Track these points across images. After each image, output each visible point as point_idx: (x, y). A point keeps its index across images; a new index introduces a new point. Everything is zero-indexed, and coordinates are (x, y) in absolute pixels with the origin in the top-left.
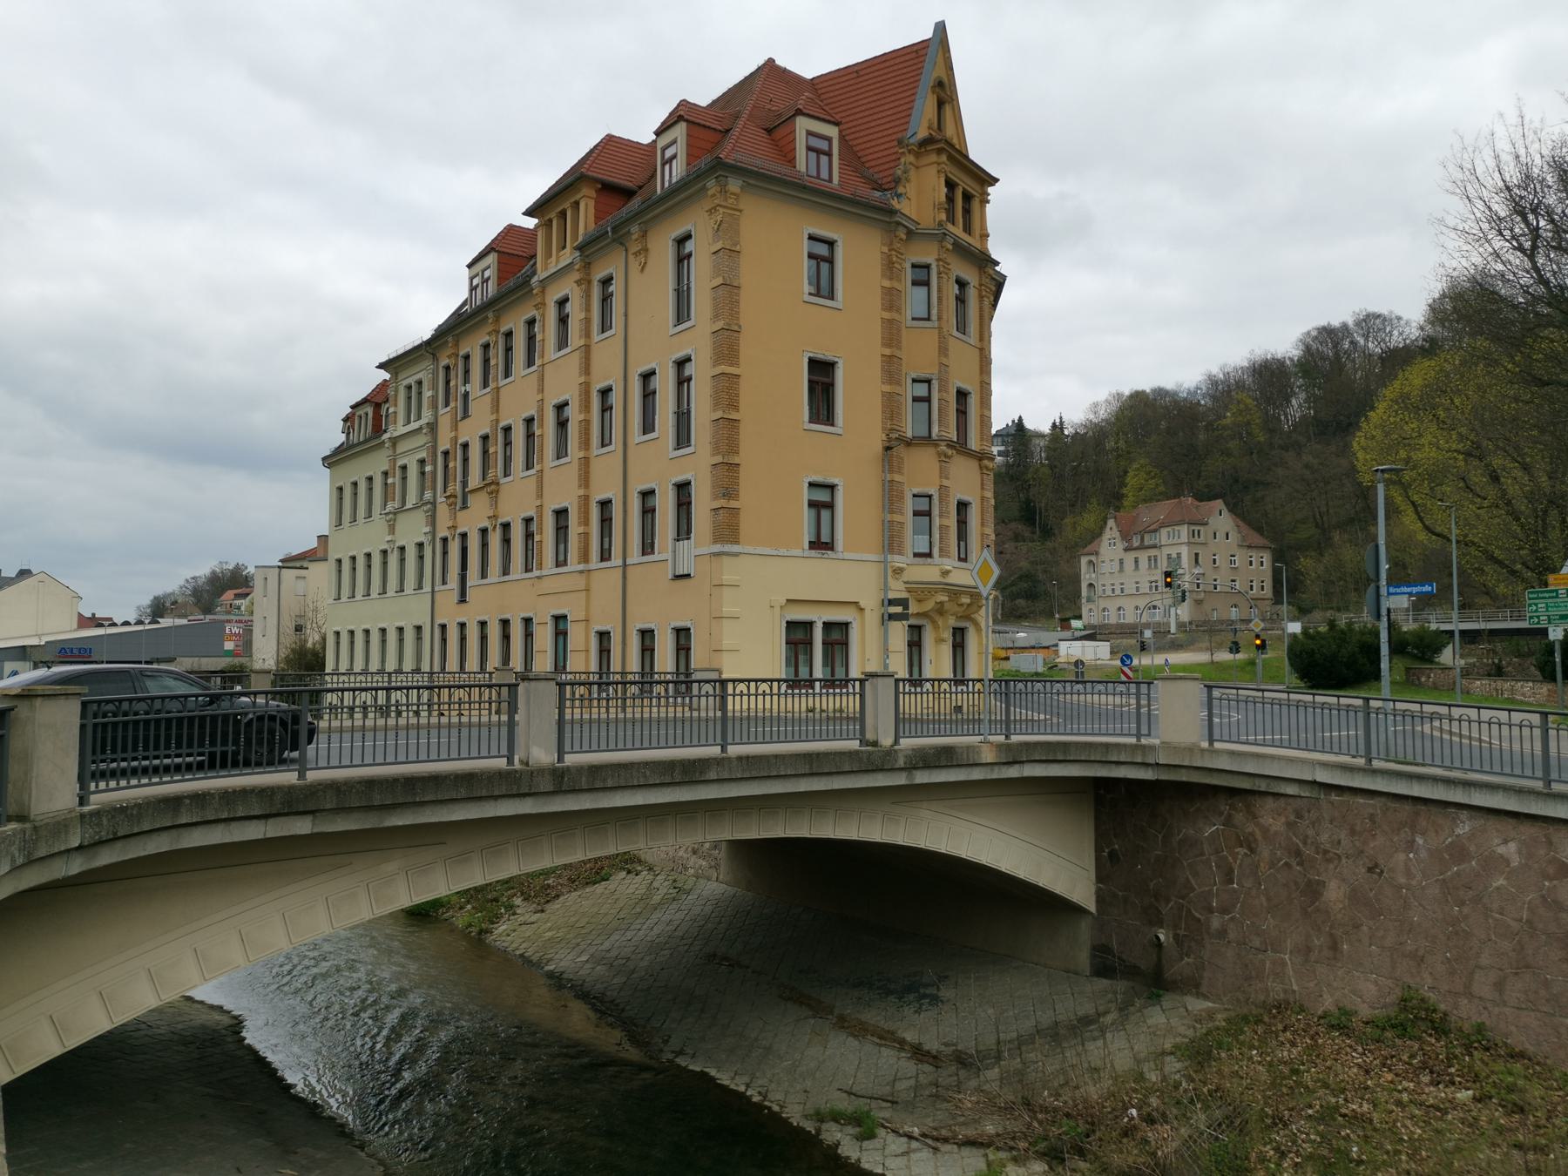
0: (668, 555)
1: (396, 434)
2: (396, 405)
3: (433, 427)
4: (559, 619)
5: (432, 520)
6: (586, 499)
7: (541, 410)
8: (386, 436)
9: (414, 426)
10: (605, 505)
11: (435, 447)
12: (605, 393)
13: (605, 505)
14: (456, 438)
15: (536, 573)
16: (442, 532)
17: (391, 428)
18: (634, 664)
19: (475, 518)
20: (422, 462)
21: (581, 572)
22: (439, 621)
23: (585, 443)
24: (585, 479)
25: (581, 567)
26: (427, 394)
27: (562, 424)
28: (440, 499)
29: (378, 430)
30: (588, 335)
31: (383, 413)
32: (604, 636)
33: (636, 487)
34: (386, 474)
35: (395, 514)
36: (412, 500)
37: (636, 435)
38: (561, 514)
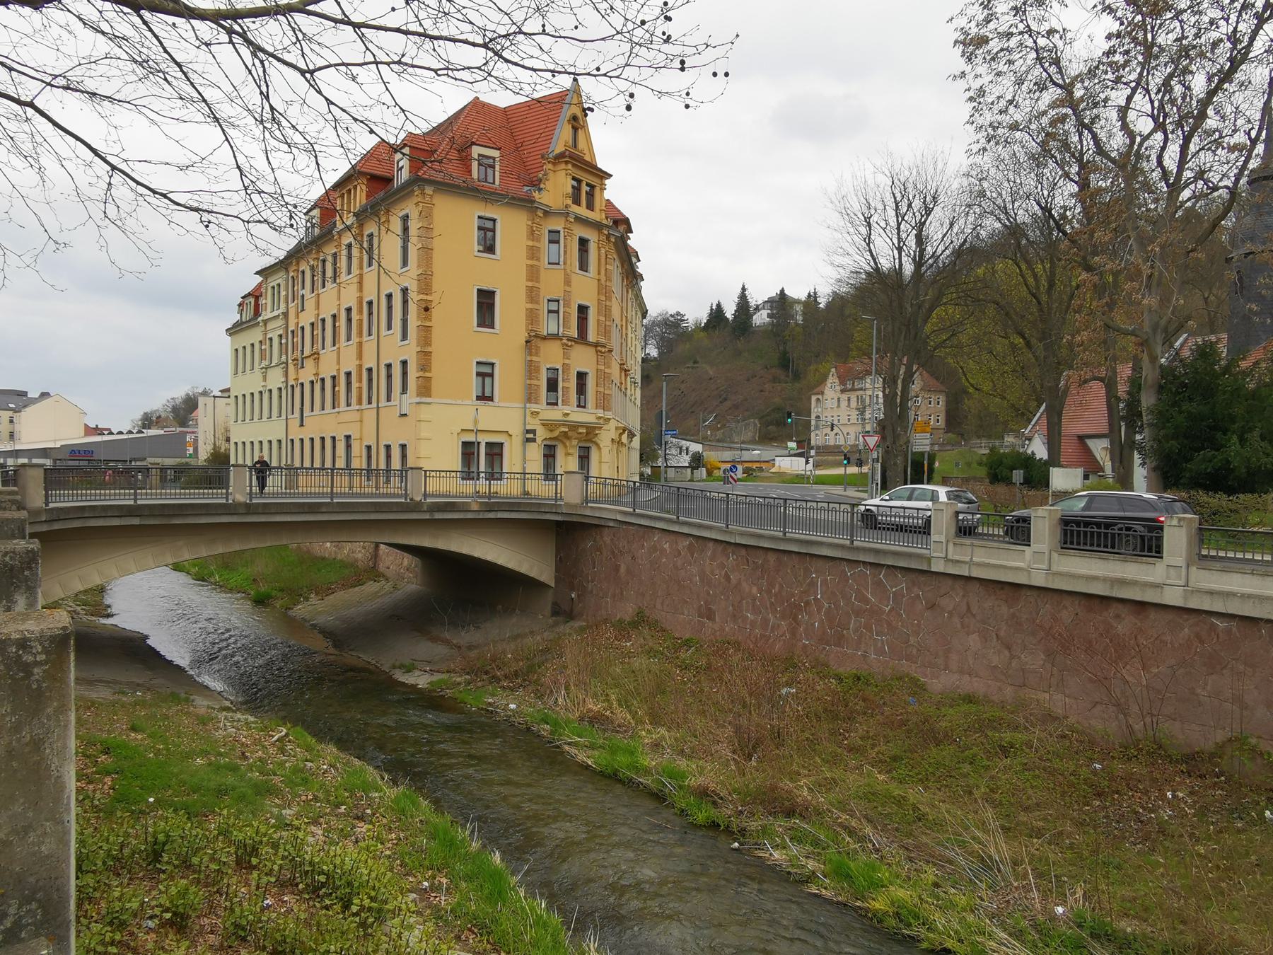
0: (397, 403)
1: (266, 318)
2: (266, 299)
3: (286, 315)
4: (348, 438)
5: (286, 375)
6: (360, 366)
7: (339, 310)
8: (260, 319)
9: (276, 313)
10: (370, 370)
11: (287, 328)
12: (370, 303)
13: (370, 370)
14: (298, 323)
15: (337, 410)
16: (291, 382)
17: (264, 313)
18: (383, 466)
19: (307, 375)
20: (280, 336)
21: (358, 410)
22: (290, 438)
23: (360, 334)
24: (360, 356)
25: (357, 407)
26: (283, 293)
27: (349, 320)
28: (290, 361)
29: (257, 313)
30: (361, 268)
31: (260, 303)
32: (369, 448)
33: (384, 362)
34: (261, 342)
35: (266, 368)
36: (275, 361)
37: (384, 332)
38: (348, 374)
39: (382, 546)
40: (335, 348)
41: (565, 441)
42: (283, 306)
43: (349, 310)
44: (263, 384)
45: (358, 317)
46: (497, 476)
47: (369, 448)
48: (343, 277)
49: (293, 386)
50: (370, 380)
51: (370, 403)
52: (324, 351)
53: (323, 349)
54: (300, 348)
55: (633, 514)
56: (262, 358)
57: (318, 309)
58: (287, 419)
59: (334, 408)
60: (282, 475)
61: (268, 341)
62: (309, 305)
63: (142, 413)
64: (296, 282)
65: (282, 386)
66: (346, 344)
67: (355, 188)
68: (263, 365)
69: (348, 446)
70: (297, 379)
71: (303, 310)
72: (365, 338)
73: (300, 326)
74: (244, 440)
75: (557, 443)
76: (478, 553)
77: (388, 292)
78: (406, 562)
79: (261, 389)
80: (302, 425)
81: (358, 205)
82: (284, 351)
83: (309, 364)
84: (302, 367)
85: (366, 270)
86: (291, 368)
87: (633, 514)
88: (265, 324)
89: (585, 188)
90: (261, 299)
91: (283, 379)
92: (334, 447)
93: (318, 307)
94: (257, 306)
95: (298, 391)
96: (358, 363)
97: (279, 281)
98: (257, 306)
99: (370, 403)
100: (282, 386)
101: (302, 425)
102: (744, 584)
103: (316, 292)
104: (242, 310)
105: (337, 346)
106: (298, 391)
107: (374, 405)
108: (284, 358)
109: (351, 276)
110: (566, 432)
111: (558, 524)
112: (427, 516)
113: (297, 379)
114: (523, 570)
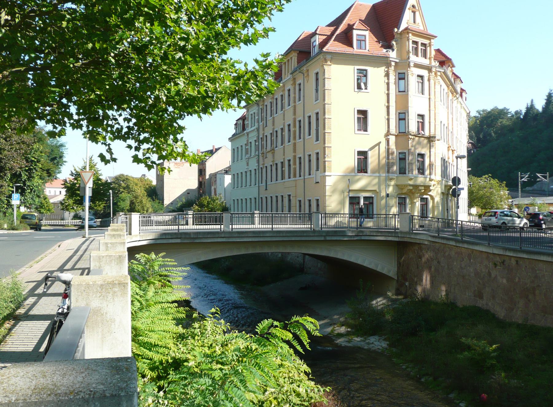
0: (314, 176)
1: (248, 131)
2: (248, 121)
3: (258, 129)
4: (289, 196)
5: (258, 162)
6: (295, 157)
7: (284, 126)
8: (245, 132)
9: (253, 128)
10: (300, 158)
11: (258, 136)
12: (300, 121)
13: (300, 158)
15: (283, 181)
16: (261, 166)
17: (247, 129)
18: (307, 212)
19: (268, 162)
20: (255, 141)
21: (294, 180)
22: (260, 196)
23: (295, 138)
24: (295, 150)
25: (294, 179)
26: (256, 118)
27: (289, 130)
28: (260, 155)
29: (244, 129)
30: (295, 102)
31: (245, 123)
32: (300, 201)
33: (307, 154)
34: (246, 144)
35: (248, 159)
36: (253, 154)
37: (307, 137)
38: (289, 161)
39: (307, 256)
40: (282, 146)
41: (411, 195)
42: (256, 124)
43: (289, 125)
44: (247, 167)
45: (293, 129)
46: (371, 216)
47: (300, 201)
48: (286, 107)
49: (262, 168)
50: (300, 163)
51: (300, 176)
52: (277, 148)
53: (277, 147)
54: (265, 147)
55: (438, 237)
56: (247, 153)
57: (274, 125)
58: (259, 186)
59: (282, 179)
60: (259, 217)
61: (249, 144)
62: (270, 123)
63: (500, 107)
64: (272, 105)
65: (256, 168)
66: (288, 144)
67: (291, 58)
68: (247, 157)
69: (290, 200)
70: (264, 164)
71: (266, 126)
72: (298, 140)
73: (265, 135)
74: (238, 198)
75: (406, 196)
76: (353, 259)
77: (308, 115)
78: (319, 265)
79: (246, 170)
80: (266, 189)
81: (293, 68)
82: (257, 149)
83: (270, 155)
84: (266, 158)
85: (297, 103)
86: (261, 158)
87: (438, 237)
88: (248, 135)
89: (420, 47)
90: (246, 121)
91: (257, 165)
92: (283, 201)
93: (273, 125)
94: (244, 125)
95: (264, 170)
96: (294, 154)
97: (255, 111)
98: (244, 125)
99: (300, 176)
100: (256, 168)
101: (266, 189)
102: (499, 278)
103: (272, 116)
104: (237, 127)
105: (283, 145)
106: (264, 170)
107: (302, 178)
108: (257, 152)
109: (290, 107)
110: (411, 190)
111: (399, 243)
112: (322, 239)
113: (264, 164)
114: (379, 269)
